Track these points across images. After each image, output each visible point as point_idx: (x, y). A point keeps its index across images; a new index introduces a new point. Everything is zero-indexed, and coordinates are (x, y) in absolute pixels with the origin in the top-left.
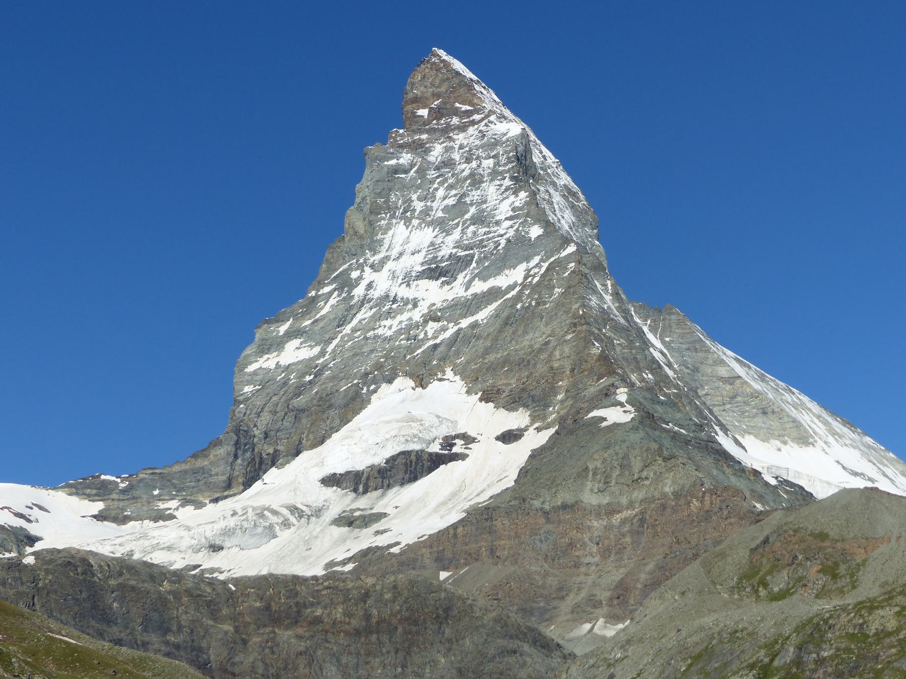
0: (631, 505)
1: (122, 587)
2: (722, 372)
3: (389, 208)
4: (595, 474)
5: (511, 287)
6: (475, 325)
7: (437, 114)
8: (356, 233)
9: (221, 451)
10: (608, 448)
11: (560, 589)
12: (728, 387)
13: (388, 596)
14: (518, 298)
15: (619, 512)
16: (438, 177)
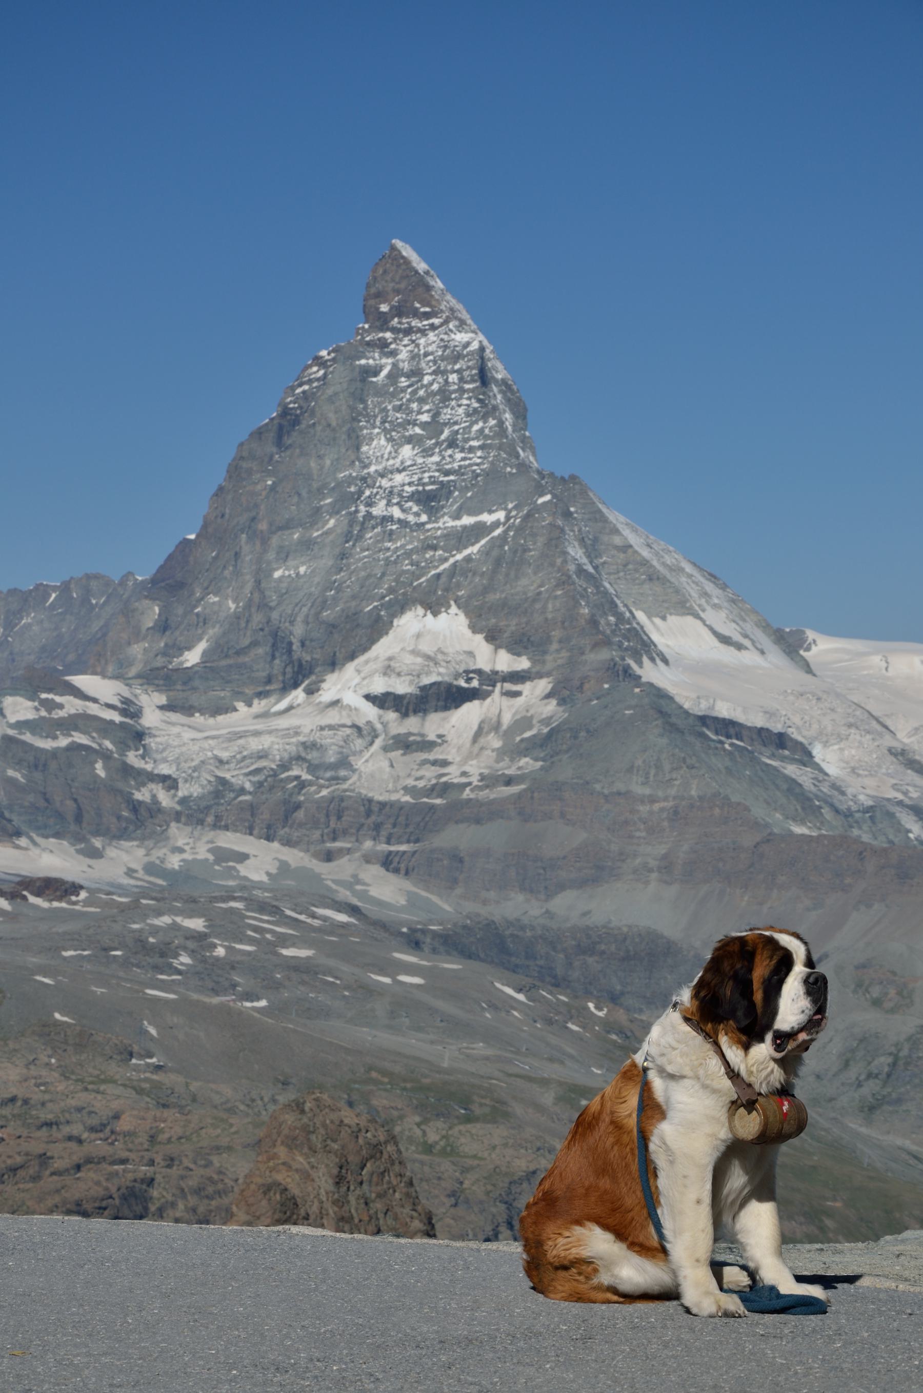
0: (666, 799)
1: (512, 935)
2: (617, 540)
3: (367, 415)
4: (638, 771)
5: (496, 524)
6: (468, 559)
7: (399, 311)
8: (329, 425)
9: (260, 651)
10: (645, 751)
11: (621, 854)
12: (622, 556)
13: (637, 940)
14: (503, 538)
15: (658, 802)
16: (409, 386)
